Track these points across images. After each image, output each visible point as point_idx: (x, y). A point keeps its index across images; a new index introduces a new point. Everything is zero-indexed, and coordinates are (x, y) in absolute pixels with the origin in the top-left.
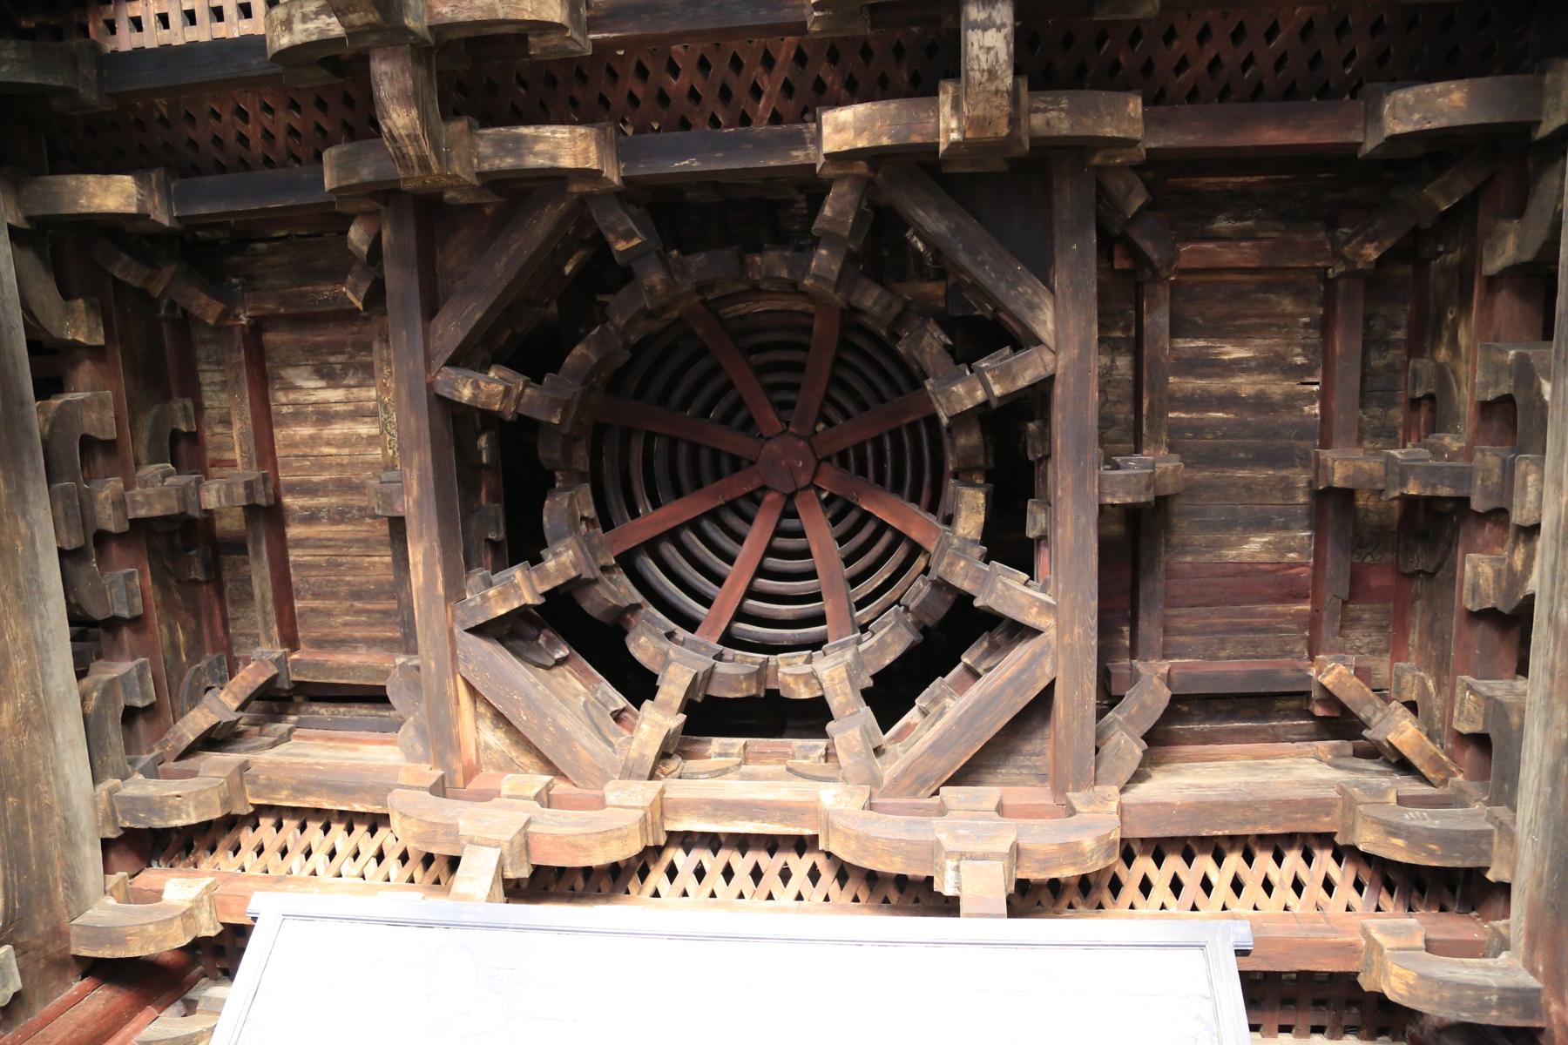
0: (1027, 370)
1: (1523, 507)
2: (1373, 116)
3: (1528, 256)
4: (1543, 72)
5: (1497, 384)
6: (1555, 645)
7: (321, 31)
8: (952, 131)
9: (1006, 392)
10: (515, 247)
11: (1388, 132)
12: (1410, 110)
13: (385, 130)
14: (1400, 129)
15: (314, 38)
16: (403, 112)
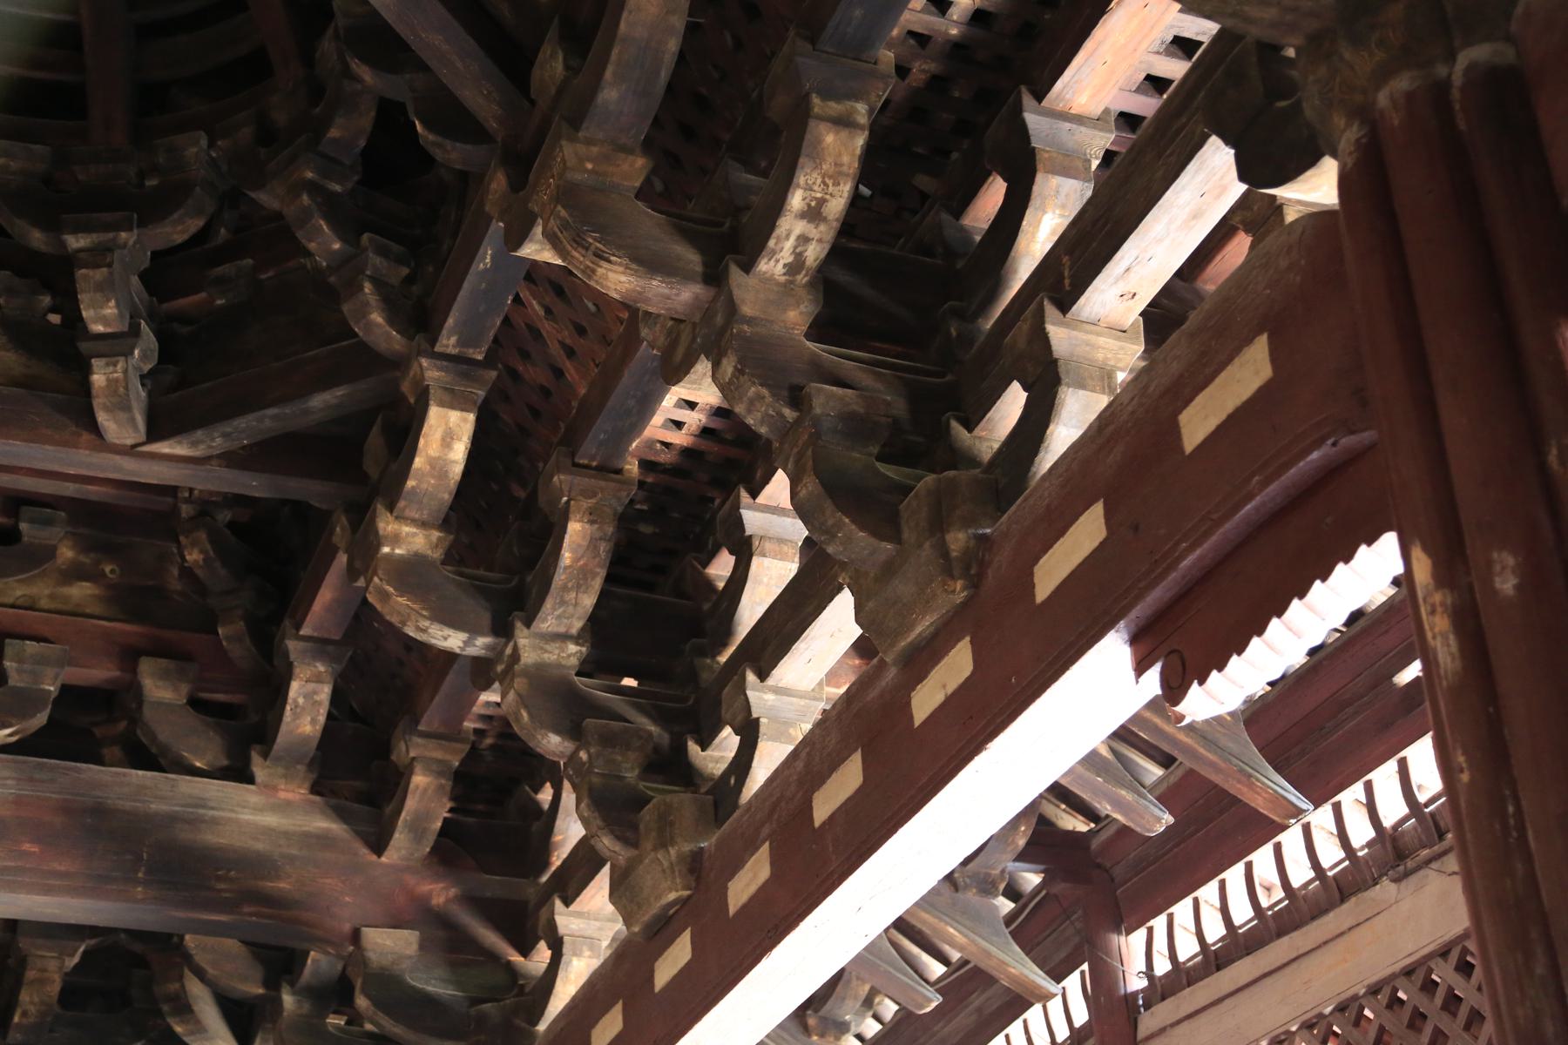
0: (120, 427)
2: (321, 647)
3: (147, 712)
4: (311, 765)
5: (19, 671)
7: (774, 252)
8: (393, 549)
9: (94, 392)
10: (459, 65)
11: (297, 671)
13: (613, 258)
14: (295, 687)
15: (771, 243)
16: (623, 288)
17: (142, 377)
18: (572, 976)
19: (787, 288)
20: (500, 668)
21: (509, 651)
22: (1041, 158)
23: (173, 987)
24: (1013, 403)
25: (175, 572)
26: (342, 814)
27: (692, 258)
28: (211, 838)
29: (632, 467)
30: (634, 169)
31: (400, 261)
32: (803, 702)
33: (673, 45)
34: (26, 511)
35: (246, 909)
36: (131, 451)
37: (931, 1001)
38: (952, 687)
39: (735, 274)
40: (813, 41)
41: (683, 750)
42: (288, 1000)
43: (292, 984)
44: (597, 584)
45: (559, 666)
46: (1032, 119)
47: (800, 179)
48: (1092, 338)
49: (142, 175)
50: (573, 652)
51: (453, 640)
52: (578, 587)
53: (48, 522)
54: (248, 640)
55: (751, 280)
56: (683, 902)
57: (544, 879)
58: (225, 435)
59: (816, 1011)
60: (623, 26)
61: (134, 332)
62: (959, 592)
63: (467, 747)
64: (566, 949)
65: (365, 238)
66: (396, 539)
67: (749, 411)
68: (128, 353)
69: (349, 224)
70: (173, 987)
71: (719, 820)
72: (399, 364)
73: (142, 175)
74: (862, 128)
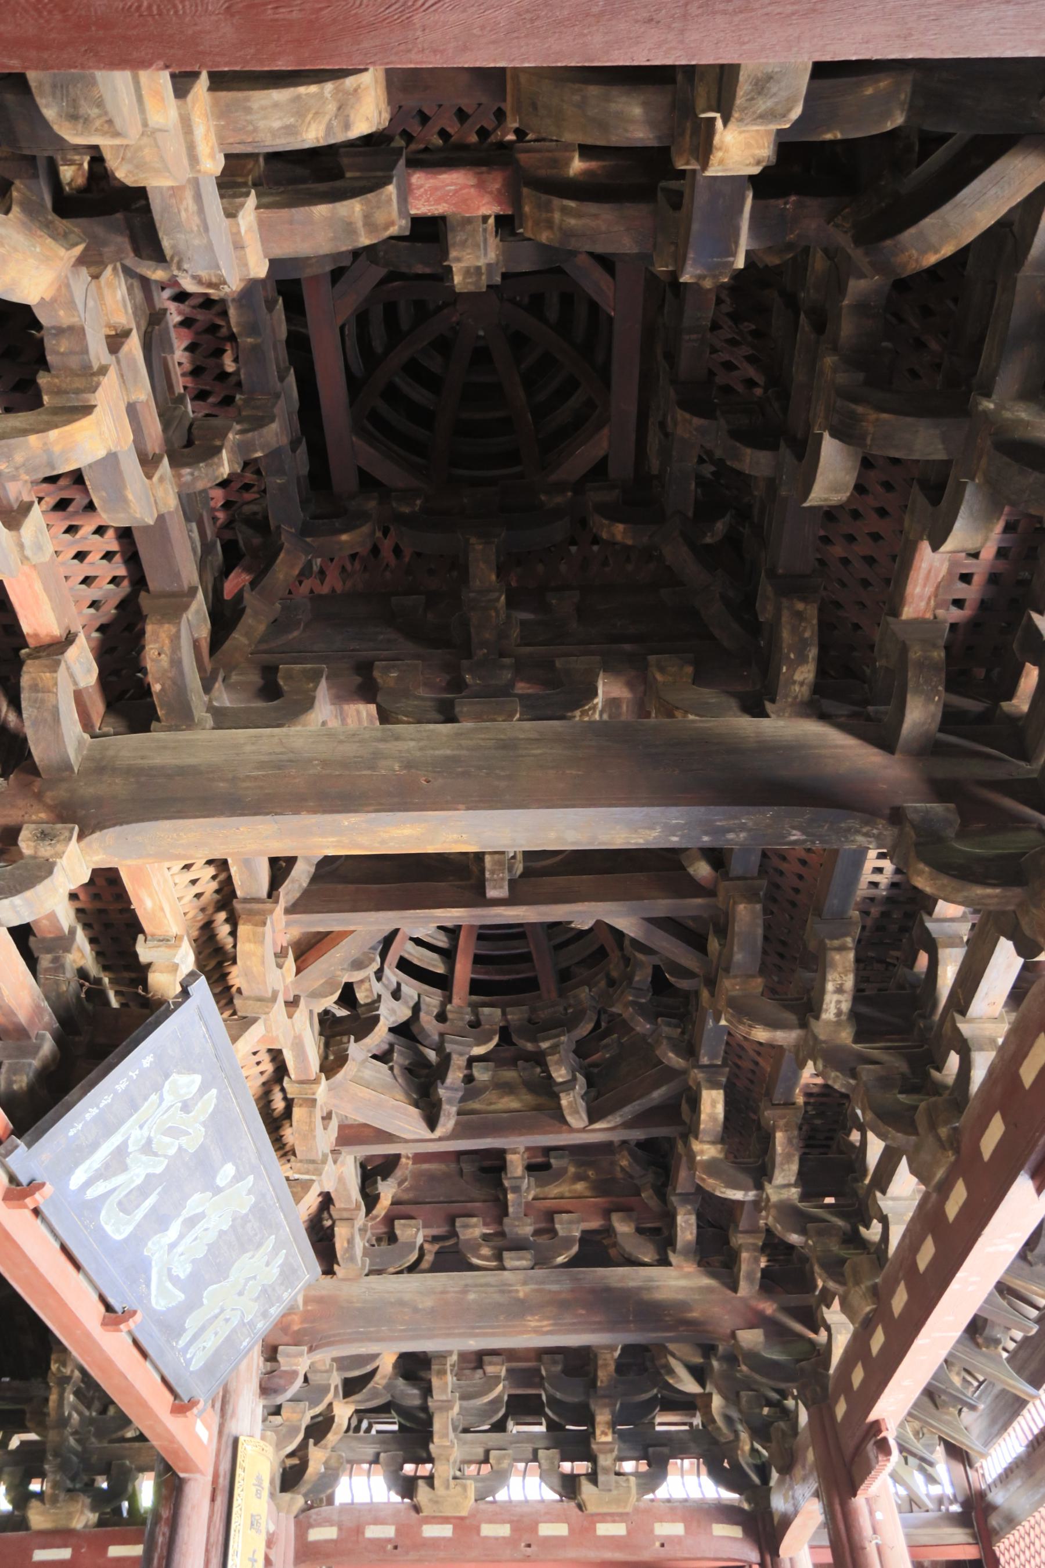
1: (512, 1259)
2: (686, 1198)
3: (620, 1240)
6: (455, 1292)
12: (686, 1222)
14: (680, 1219)
15: (824, 1006)
17: (582, 1098)
18: (840, 1344)
19: (838, 1024)
20: (763, 1204)
21: (764, 1196)
22: (939, 941)
23: (663, 1361)
24: (954, 1060)
25: (618, 1169)
26: (713, 1275)
27: (792, 1018)
28: (660, 1296)
29: (800, 1100)
30: (758, 984)
31: (676, 1026)
32: (907, 1202)
33: (760, 931)
34: (552, 1153)
35: (681, 1329)
36: (584, 1130)
37: (1031, 1328)
38: (961, 1202)
39: (812, 1021)
40: (820, 916)
41: (857, 1232)
42: (715, 1364)
43: (715, 1355)
44: (796, 1159)
45: (789, 1199)
46: (930, 925)
47: (829, 977)
48: (981, 1025)
49: (566, 1009)
50: (794, 1193)
51: (737, 1195)
52: (788, 1162)
53: (562, 1157)
54: (655, 1197)
55: (820, 1023)
56: (874, 1311)
57: (817, 1293)
58: (621, 1116)
59: (981, 1334)
60: (736, 929)
61: (574, 1079)
62: (951, 1157)
63: (763, 1235)
64: (833, 1331)
65: (659, 1020)
66: (702, 1152)
67: (835, 1082)
68: (573, 1088)
69: (653, 1014)
70: (663, 1361)
71: (881, 1266)
72: (684, 1072)
73: (566, 1009)
74: (849, 949)
